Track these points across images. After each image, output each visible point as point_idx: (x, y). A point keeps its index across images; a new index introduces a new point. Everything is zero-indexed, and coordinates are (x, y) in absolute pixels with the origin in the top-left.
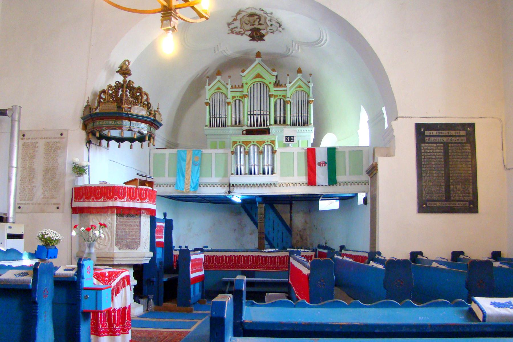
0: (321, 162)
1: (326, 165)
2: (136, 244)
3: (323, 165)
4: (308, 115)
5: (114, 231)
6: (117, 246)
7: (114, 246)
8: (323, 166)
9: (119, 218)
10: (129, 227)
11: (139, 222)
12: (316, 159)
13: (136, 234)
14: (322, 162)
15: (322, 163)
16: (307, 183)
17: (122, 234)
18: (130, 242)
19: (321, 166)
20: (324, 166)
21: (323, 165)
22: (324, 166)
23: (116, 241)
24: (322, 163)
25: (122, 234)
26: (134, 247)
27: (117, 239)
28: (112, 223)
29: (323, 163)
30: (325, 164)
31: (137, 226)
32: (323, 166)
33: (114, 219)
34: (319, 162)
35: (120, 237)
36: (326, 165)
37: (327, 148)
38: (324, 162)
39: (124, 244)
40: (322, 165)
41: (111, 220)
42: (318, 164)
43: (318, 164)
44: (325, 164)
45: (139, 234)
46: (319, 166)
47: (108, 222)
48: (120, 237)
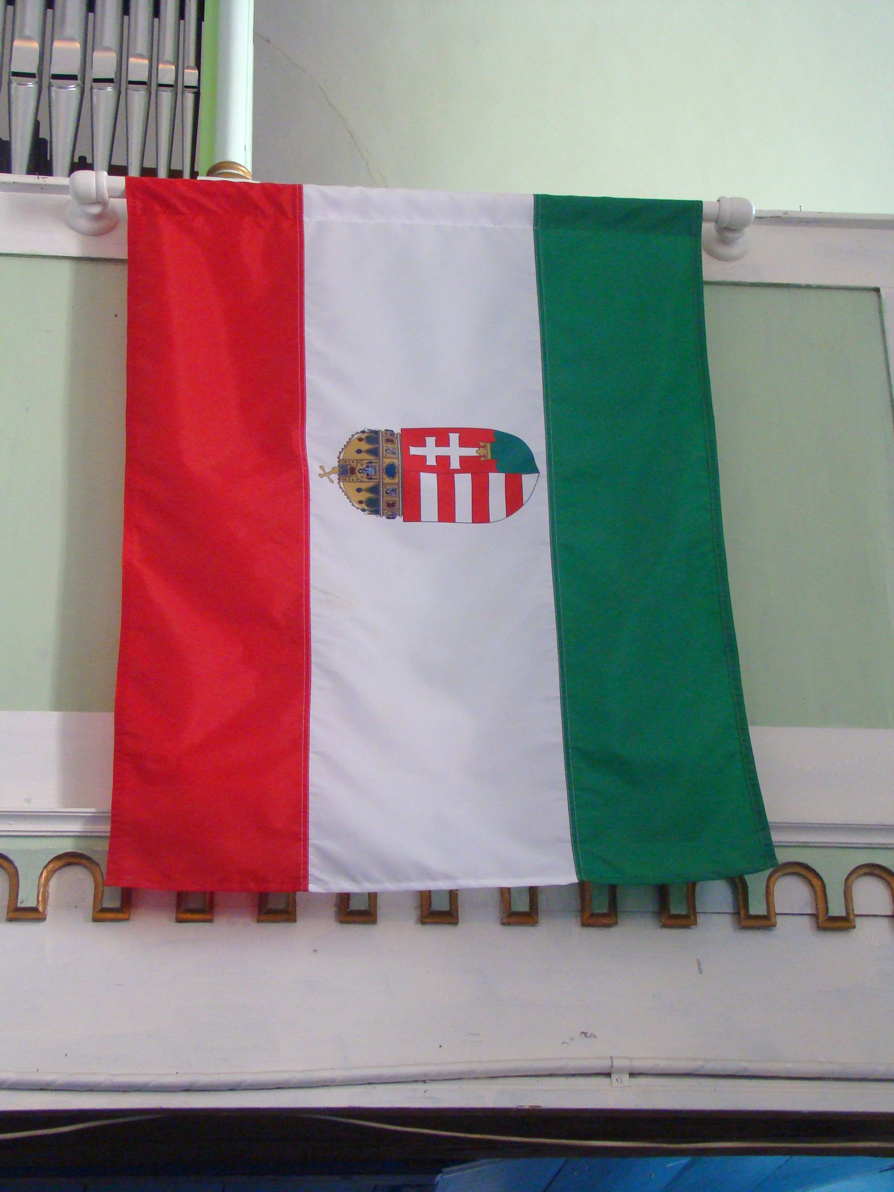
0: (416, 436)
1: (514, 502)
3: (463, 484)
4: (190, 77)
8: (447, 513)
12: (311, 376)
14: (442, 436)
15: (430, 451)
16: (100, 850)
19: (412, 513)
20: (481, 514)
21: (463, 484)
22: (481, 514)
24: (430, 451)
29: (455, 452)
30: (497, 482)
32: (447, 513)
34: (372, 437)
36: (514, 502)
37: (532, 201)
38: (469, 436)
40: (429, 483)
42: (346, 471)
43: (346, 471)
44: (497, 482)
46: (373, 506)
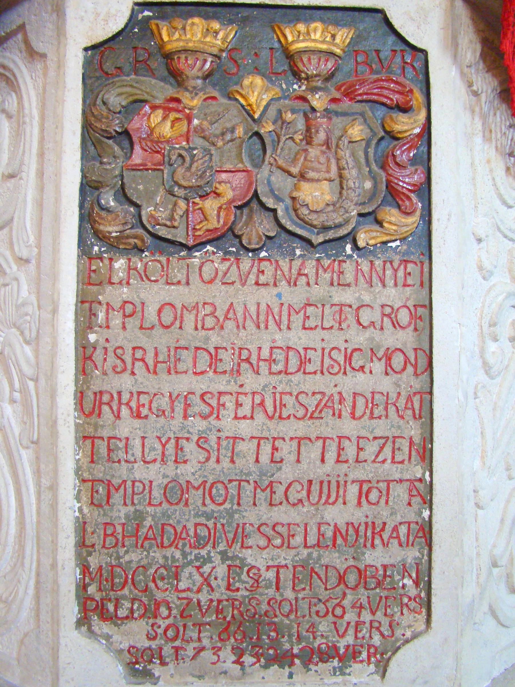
2: (363, 595)
5: (54, 434)
6: (106, 628)
7: (56, 622)
9: (120, 264)
10: (264, 379)
11: (404, 317)
13: (359, 474)
17: (170, 469)
18: (286, 575)
23: (85, 569)
25: (170, 469)
26: (342, 645)
27: (96, 539)
28: (37, 337)
31: (378, 367)
33: (55, 277)
35: (140, 516)
39: (204, 597)
41: (33, 298)
45: (418, 471)
47: (14, 325)
48: (140, 516)
